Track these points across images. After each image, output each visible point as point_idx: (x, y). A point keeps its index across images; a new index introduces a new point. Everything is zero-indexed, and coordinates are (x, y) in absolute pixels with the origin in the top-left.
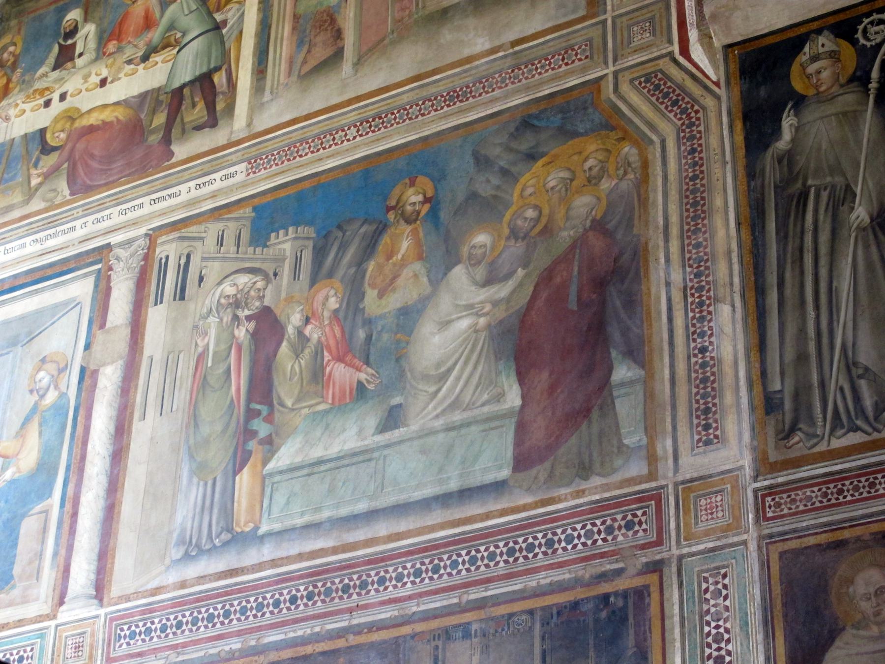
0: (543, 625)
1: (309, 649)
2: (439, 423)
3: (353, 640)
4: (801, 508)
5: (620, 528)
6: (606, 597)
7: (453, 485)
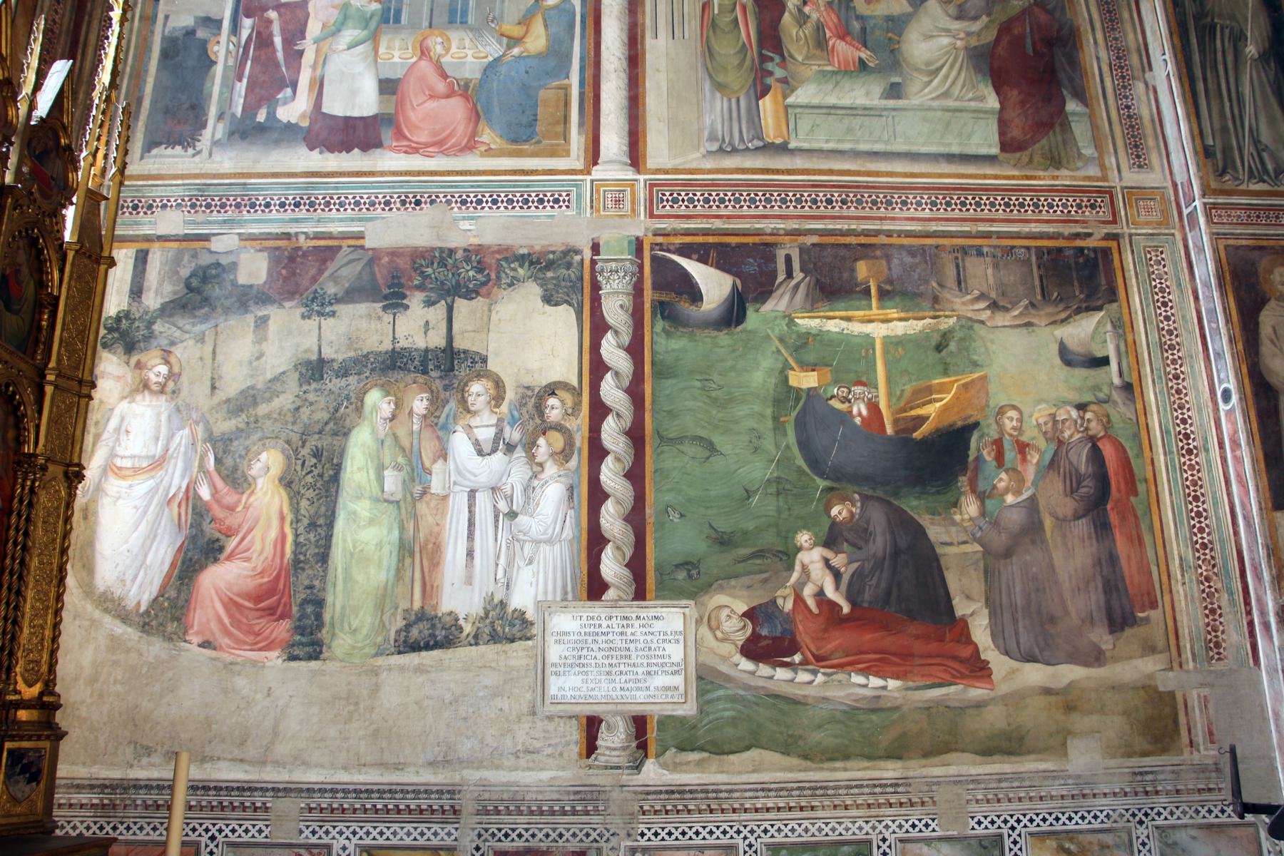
0: (1037, 258)
1: (848, 240)
2: (935, 104)
3: (883, 240)
4: (1235, 221)
5: (1086, 206)
6: (1081, 249)
7: (955, 150)
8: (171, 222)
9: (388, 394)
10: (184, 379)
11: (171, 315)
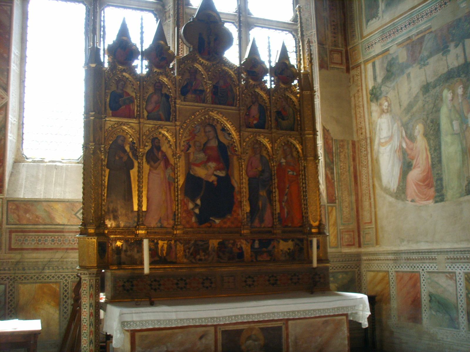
8: (378, 49)
9: (449, 90)
10: (392, 105)
11: (385, 83)
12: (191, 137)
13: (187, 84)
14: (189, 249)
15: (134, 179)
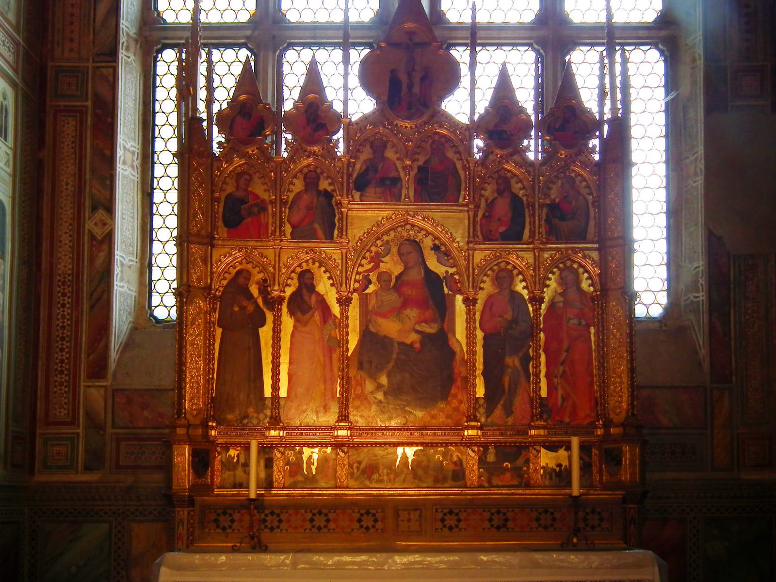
12: (372, 264)
13: (367, 170)
14: (360, 463)
15: (266, 344)
